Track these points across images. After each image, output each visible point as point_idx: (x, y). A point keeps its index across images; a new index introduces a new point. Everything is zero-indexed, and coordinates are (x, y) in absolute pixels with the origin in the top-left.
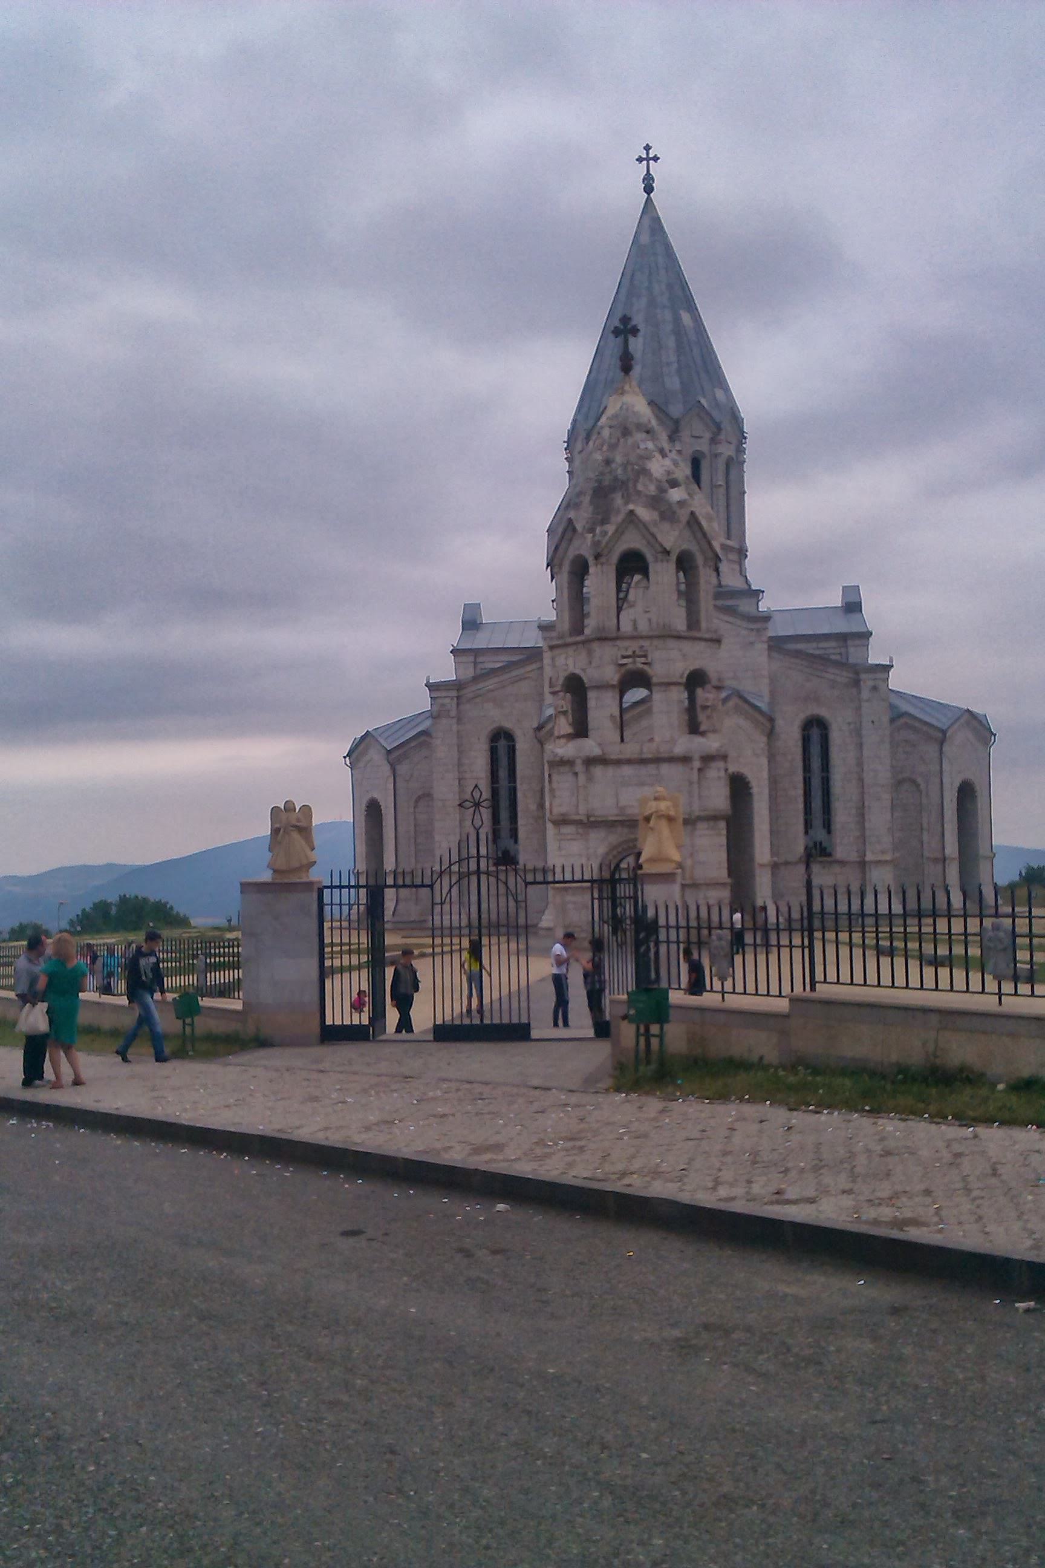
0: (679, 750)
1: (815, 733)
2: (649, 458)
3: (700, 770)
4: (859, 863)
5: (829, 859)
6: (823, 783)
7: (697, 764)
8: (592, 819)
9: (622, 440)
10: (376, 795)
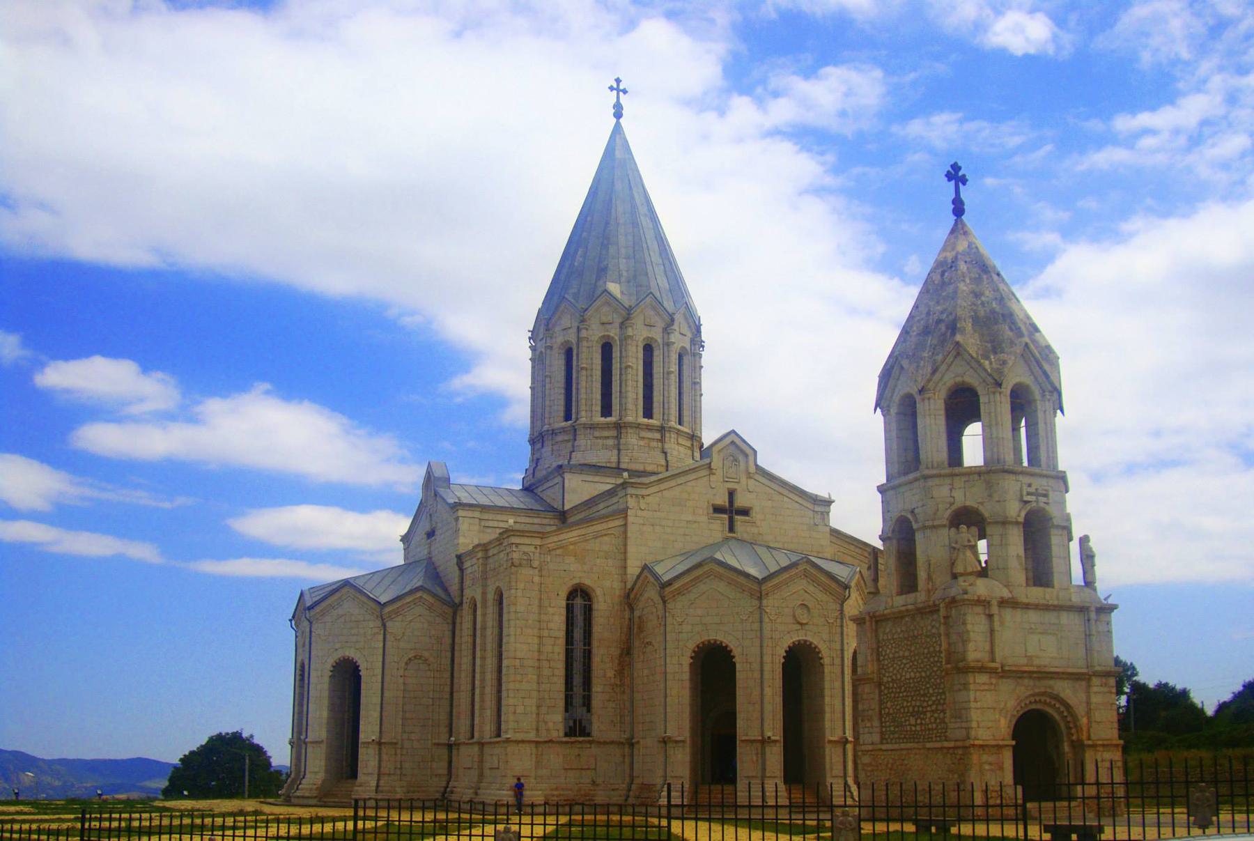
7: (1093, 615)
10: (350, 653)
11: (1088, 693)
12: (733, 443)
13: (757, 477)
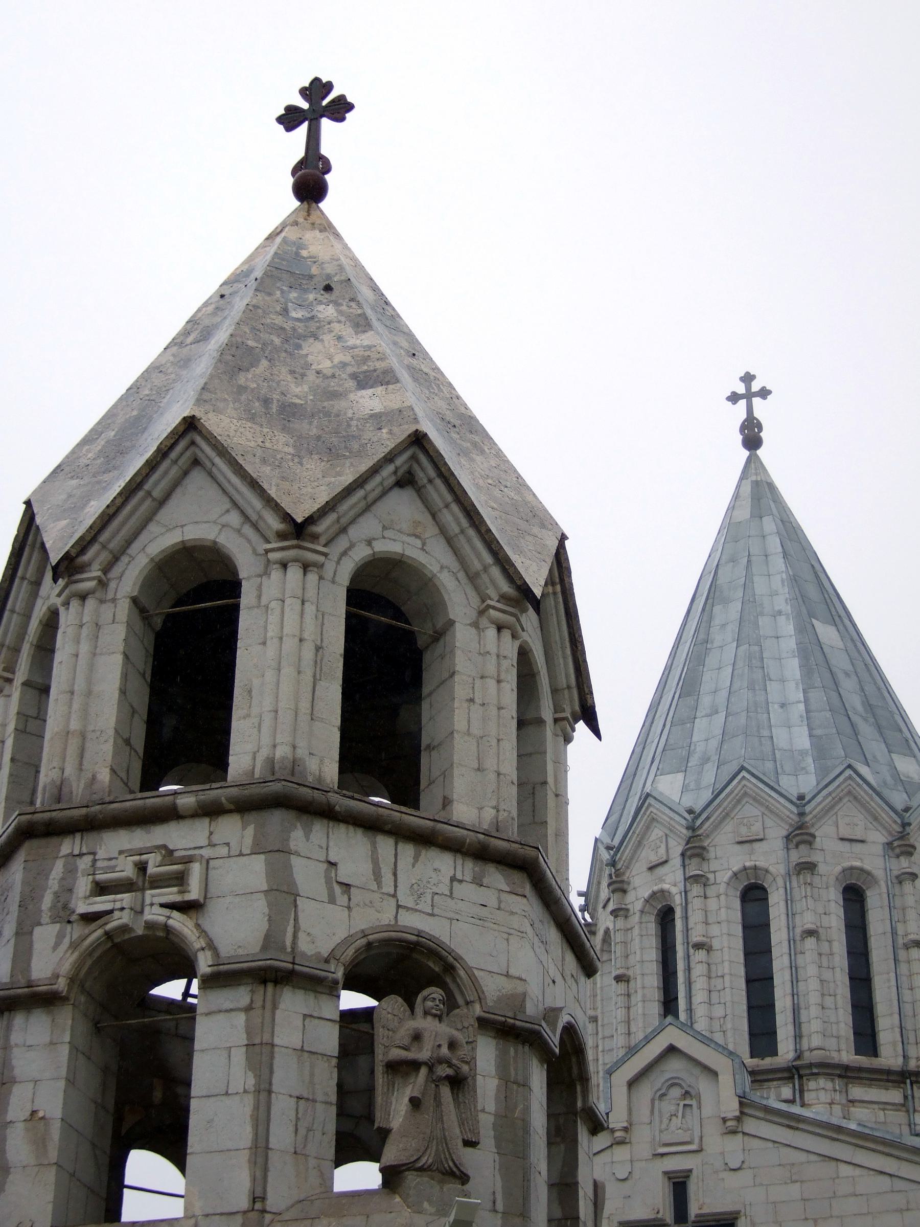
12: (672, 1050)
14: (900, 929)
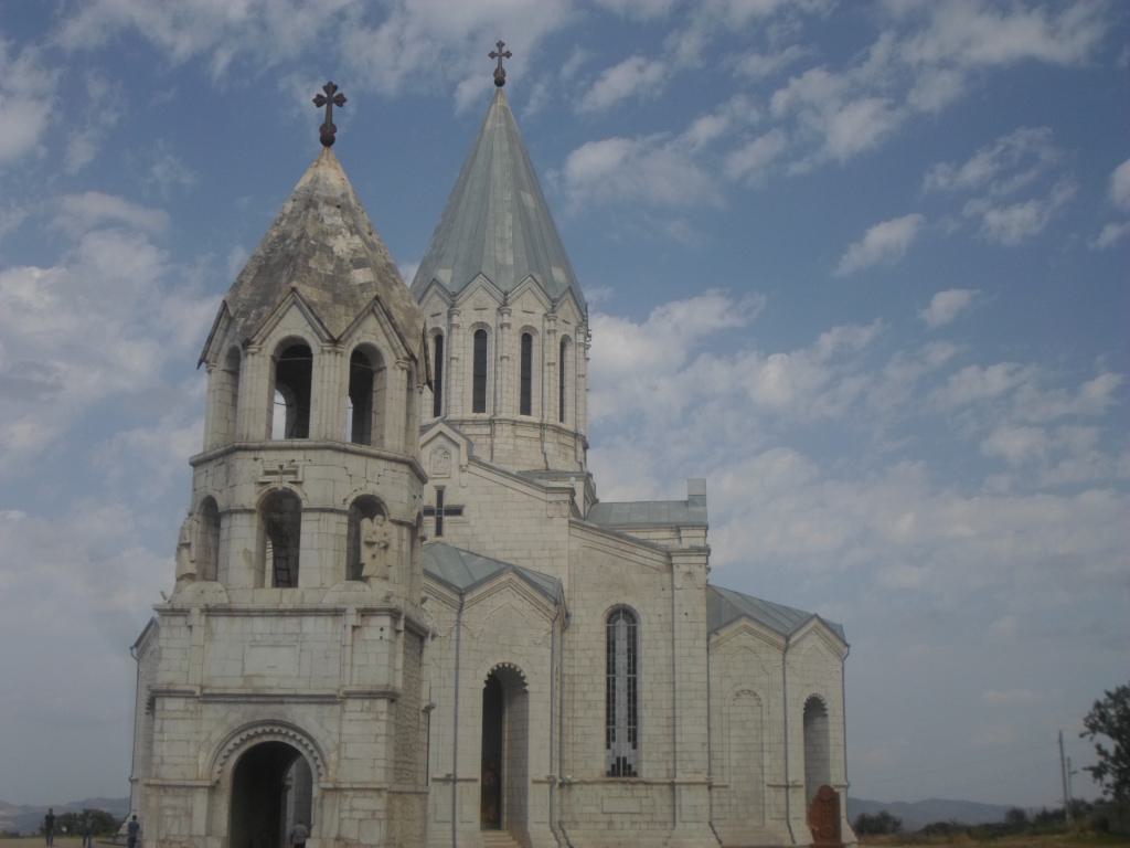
0: (330, 600)
1: (622, 624)
2: (336, 232)
3: (354, 628)
4: (669, 784)
5: (633, 779)
6: (629, 687)
7: (353, 620)
8: (207, 691)
9: (304, 213)
11: (341, 720)
12: (441, 433)
13: (472, 468)
14: (546, 356)
